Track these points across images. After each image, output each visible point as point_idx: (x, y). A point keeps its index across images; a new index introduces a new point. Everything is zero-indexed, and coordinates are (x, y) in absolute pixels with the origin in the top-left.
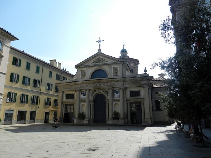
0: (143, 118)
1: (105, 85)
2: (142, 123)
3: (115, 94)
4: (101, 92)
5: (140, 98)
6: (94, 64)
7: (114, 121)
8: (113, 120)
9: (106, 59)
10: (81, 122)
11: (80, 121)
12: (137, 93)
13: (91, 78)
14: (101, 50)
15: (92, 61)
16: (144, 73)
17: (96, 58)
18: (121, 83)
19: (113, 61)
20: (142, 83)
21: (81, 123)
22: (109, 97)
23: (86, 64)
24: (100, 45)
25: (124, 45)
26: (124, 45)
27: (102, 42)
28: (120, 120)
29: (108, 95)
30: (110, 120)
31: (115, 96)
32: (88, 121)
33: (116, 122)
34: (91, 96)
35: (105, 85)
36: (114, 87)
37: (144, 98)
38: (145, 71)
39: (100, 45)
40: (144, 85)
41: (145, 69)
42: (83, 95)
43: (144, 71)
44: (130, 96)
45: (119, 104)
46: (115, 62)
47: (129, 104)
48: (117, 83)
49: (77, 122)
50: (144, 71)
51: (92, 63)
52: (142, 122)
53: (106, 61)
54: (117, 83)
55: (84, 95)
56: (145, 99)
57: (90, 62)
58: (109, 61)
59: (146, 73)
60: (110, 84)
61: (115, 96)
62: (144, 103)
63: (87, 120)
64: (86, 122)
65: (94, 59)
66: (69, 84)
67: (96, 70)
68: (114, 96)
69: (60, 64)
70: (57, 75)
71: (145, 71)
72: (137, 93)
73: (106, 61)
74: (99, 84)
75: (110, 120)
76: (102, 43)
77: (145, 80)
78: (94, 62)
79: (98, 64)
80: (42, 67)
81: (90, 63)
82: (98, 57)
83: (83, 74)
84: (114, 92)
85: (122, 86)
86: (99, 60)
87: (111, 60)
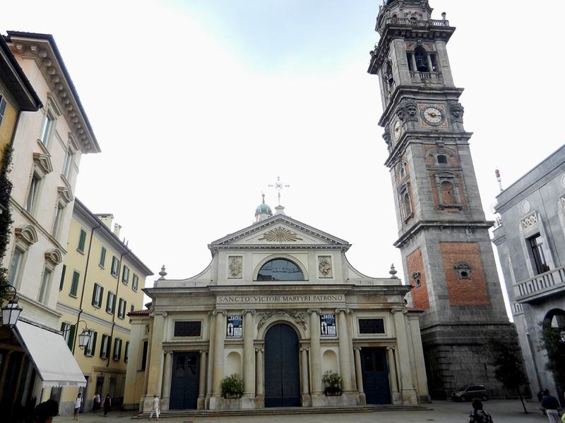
0: (394, 388)
1: (300, 299)
2: (395, 403)
3: (324, 326)
4: (287, 318)
5: (385, 337)
6: (265, 242)
7: (329, 397)
8: (326, 395)
9: (300, 234)
10: (234, 405)
11: (228, 402)
12: (377, 326)
13: (260, 277)
14: (283, 208)
15: (260, 234)
16: (391, 276)
17: (272, 228)
18: (340, 298)
19: (318, 242)
20: (389, 301)
21: (231, 407)
22: (311, 330)
23: (243, 242)
24: (279, 196)
25: (263, 196)
26: (263, 196)
27: (284, 188)
28: (344, 396)
29: (305, 328)
30: (319, 395)
31: (324, 330)
32: (253, 402)
33: (333, 401)
34: (259, 328)
35: (300, 299)
36: (323, 307)
37: (395, 339)
38: (393, 272)
39: (279, 196)
40: (395, 307)
41: (393, 267)
42: (234, 327)
43: (391, 273)
44: (360, 333)
45: (335, 351)
46: (323, 243)
47: (358, 353)
48: (329, 298)
49: (219, 405)
50: (391, 273)
51: (260, 239)
52: (394, 399)
53: (298, 239)
54: (329, 298)
55: (237, 324)
56: (398, 340)
57: (253, 236)
58: (308, 240)
59: (396, 278)
60: (312, 297)
61: (324, 330)
62: (394, 351)
63: (250, 400)
64: (246, 404)
65: (266, 231)
66: (190, 293)
67: (273, 258)
68: (323, 332)
69: (120, 227)
70: (114, 258)
71: (393, 272)
72: (377, 326)
73: (298, 239)
74: (281, 298)
75: (319, 395)
76: (284, 191)
77: (396, 295)
78: (266, 237)
79: (278, 243)
80: (91, 233)
81: (254, 240)
82: (277, 226)
83: (235, 271)
84: (321, 321)
85: (342, 306)
86: (280, 235)
87: (314, 239)
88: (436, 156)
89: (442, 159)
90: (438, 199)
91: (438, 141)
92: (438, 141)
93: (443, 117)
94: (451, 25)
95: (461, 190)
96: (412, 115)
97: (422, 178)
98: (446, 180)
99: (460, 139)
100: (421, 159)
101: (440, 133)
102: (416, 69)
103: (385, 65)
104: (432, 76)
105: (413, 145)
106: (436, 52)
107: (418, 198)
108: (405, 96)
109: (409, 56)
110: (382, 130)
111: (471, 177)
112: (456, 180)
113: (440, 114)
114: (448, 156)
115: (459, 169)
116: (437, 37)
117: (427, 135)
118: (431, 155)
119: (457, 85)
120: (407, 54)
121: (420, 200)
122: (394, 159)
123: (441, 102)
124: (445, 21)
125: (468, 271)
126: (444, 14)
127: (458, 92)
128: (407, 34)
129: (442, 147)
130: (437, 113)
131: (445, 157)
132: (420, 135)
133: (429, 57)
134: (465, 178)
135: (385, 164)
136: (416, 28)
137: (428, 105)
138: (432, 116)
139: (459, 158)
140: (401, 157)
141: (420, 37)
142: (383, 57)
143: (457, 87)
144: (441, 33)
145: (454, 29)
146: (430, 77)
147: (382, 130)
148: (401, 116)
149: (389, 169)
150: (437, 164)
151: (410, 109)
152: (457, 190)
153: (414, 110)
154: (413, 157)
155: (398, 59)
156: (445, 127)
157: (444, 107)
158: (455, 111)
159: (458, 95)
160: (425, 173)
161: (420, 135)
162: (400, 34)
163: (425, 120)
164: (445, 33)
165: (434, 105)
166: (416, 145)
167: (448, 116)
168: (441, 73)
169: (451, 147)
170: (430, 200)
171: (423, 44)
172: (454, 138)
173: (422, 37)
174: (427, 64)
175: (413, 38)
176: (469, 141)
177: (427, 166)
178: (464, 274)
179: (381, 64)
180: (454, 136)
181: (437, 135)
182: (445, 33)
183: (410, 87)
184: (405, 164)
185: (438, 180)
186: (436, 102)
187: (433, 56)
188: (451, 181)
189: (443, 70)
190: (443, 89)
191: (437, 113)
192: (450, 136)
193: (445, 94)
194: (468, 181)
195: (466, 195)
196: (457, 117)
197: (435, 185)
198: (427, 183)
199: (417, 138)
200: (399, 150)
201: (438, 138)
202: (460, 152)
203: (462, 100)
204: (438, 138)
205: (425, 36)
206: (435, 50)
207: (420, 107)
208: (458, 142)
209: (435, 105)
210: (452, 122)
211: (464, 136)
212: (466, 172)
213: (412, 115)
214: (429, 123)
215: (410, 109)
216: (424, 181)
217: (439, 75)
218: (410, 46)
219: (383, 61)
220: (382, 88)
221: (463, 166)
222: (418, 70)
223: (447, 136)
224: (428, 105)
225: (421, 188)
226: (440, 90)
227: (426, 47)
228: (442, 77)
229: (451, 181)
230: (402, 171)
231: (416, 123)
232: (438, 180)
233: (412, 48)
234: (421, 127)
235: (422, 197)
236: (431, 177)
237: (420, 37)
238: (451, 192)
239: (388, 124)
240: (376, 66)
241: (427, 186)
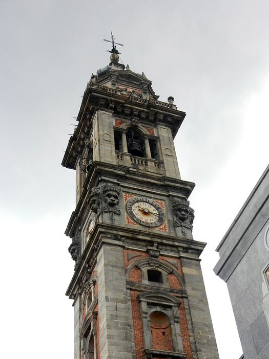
88: (145, 270)
89: (154, 276)
90: (143, 340)
91: (149, 248)
92: (149, 248)
93: (161, 220)
94: (180, 106)
95: (184, 331)
96: (112, 205)
97: (117, 301)
98: (158, 309)
99: (186, 250)
100: (120, 270)
101: (154, 236)
102: (125, 150)
103: (86, 151)
104: (149, 163)
105: (108, 247)
106: (158, 138)
107: (106, 334)
108: (103, 178)
109: (118, 135)
110: (69, 241)
111: (201, 310)
112: (177, 311)
113: (156, 212)
114: (164, 273)
115: (183, 295)
116: (160, 121)
117: (132, 236)
118: (137, 268)
119: (184, 176)
120: (115, 132)
121: (109, 337)
122: (80, 280)
123: (159, 197)
124: (172, 105)
126: (171, 99)
127: (187, 188)
128: (119, 108)
129: (157, 257)
130: (152, 209)
131: (160, 273)
132: (121, 233)
133: (147, 142)
134: (193, 311)
135: (67, 294)
136: (131, 103)
137: (139, 198)
138: (146, 213)
139: (182, 279)
140: (90, 273)
141: (135, 116)
142: (83, 140)
143: (183, 178)
144: (166, 116)
145: (183, 115)
146: (146, 165)
147: (69, 241)
148: (95, 206)
149: (73, 301)
150: (146, 282)
151: (109, 196)
152: (177, 328)
153: (116, 197)
154: (105, 265)
155: (101, 132)
156: (164, 230)
157: (165, 205)
158: (180, 210)
159: (188, 192)
160: (123, 293)
161: (121, 233)
162: (106, 106)
163: (131, 215)
164: (174, 120)
165: (151, 200)
166: (113, 247)
167: (169, 217)
168: (163, 163)
169: (169, 260)
170: (126, 339)
171: (140, 125)
172: (176, 247)
173: (139, 116)
174: (144, 150)
175: (127, 115)
176: (200, 258)
177: (128, 283)
179: (81, 152)
180: (177, 244)
181: (149, 239)
182: (174, 120)
183: (113, 167)
184: (95, 282)
185: (144, 306)
186: (152, 196)
187: (154, 142)
188: (168, 313)
189: (166, 159)
190: (165, 179)
191: (152, 209)
192: (170, 243)
193: (166, 187)
194: (196, 316)
195: (192, 339)
196: (183, 219)
197: (138, 315)
198: (126, 311)
199: (116, 237)
200: (88, 262)
201: (151, 243)
202: (186, 270)
203: (194, 201)
204: (151, 243)
205: (143, 116)
206: (156, 135)
207: (125, 199)
208: (183, 255)
209: (151, 200)
210: (175, 225)
211: (193, 247)
212: (193, 301)
213: (112, 205)
214: (138, 222)
215: (109, 196)
216: (120, 305)
217: (160, 164)
218: (121, 123)
219: (83, 147)
220: (79, 183)
221: (189, 291)
222: (129, 150)
223: (165, 241)
224: (139, 198)
225: (113, 317)
226: (159, 180)
227: (144, 130)
228: (164, 167)
229: (168, 313)
230: (90, 299)
231: (116, 217)
232: (144, 306)
233: (124, 126)
234: (123, 221)
235: (114, 332)
236: (132, 301)
237: (135, 116)
238: (167, 332)
239: (80, 230)
240: (74, 154)
241: (123, 314)
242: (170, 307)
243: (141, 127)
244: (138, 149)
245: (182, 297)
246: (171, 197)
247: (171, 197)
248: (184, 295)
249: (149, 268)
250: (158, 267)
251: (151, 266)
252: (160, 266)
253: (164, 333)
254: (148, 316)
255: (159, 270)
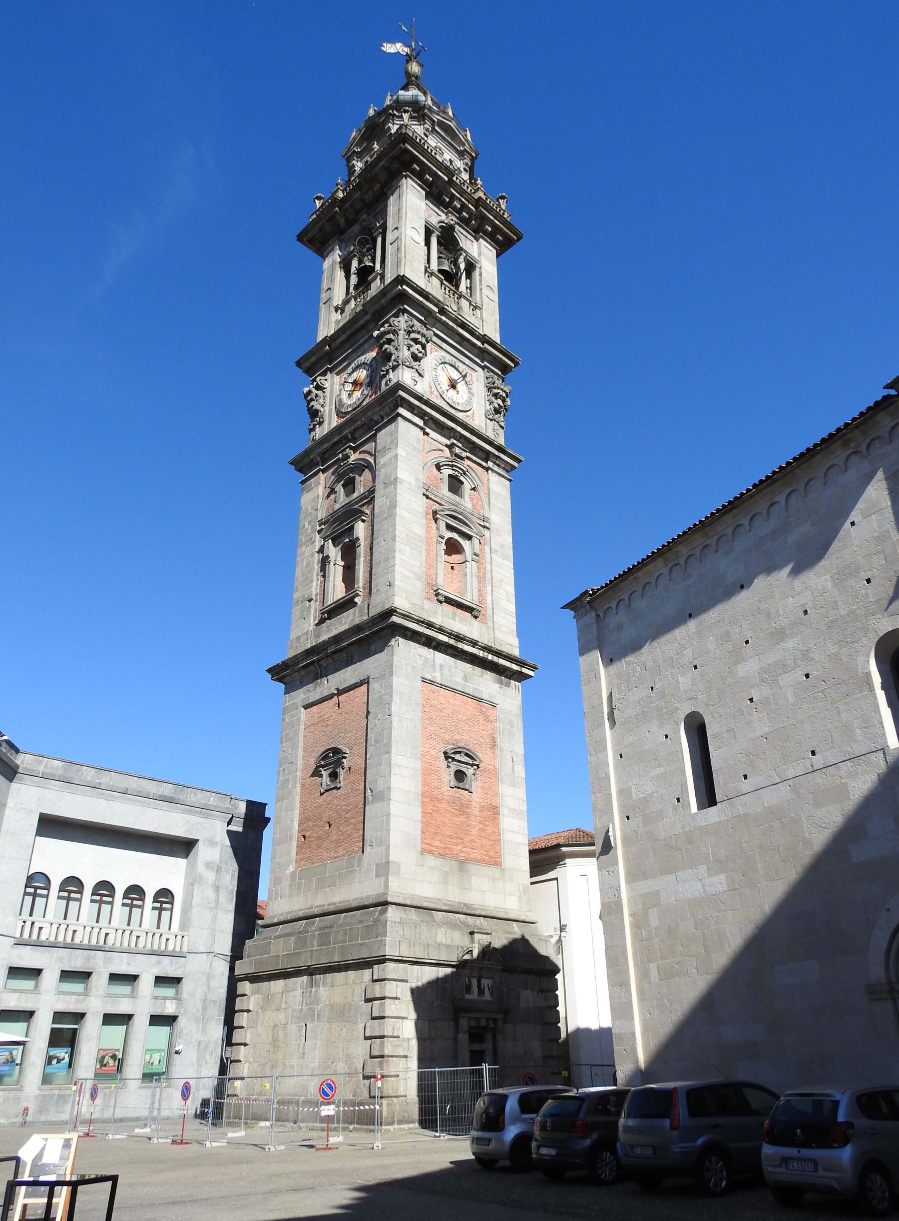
89: (455, 485)
96: (416, 358)
116: (486, 233)
125: (469, 771)
131: (462, 483)
178: (460, 776)
224: (448, 358)
229: (465, 544)
237: (455, 208)
242: (469, 538)
243: (459, 233)
244: (448, 269)
245: (484, 527)
246: (486, 370)
247: (486, 370)
248: (487, 525)
249: (451, 472)
250: (461, 475)
251: (453, 470)
252: (465, 473)
253: (452, 568)
254: (444, 541)
255: (462, 478)
